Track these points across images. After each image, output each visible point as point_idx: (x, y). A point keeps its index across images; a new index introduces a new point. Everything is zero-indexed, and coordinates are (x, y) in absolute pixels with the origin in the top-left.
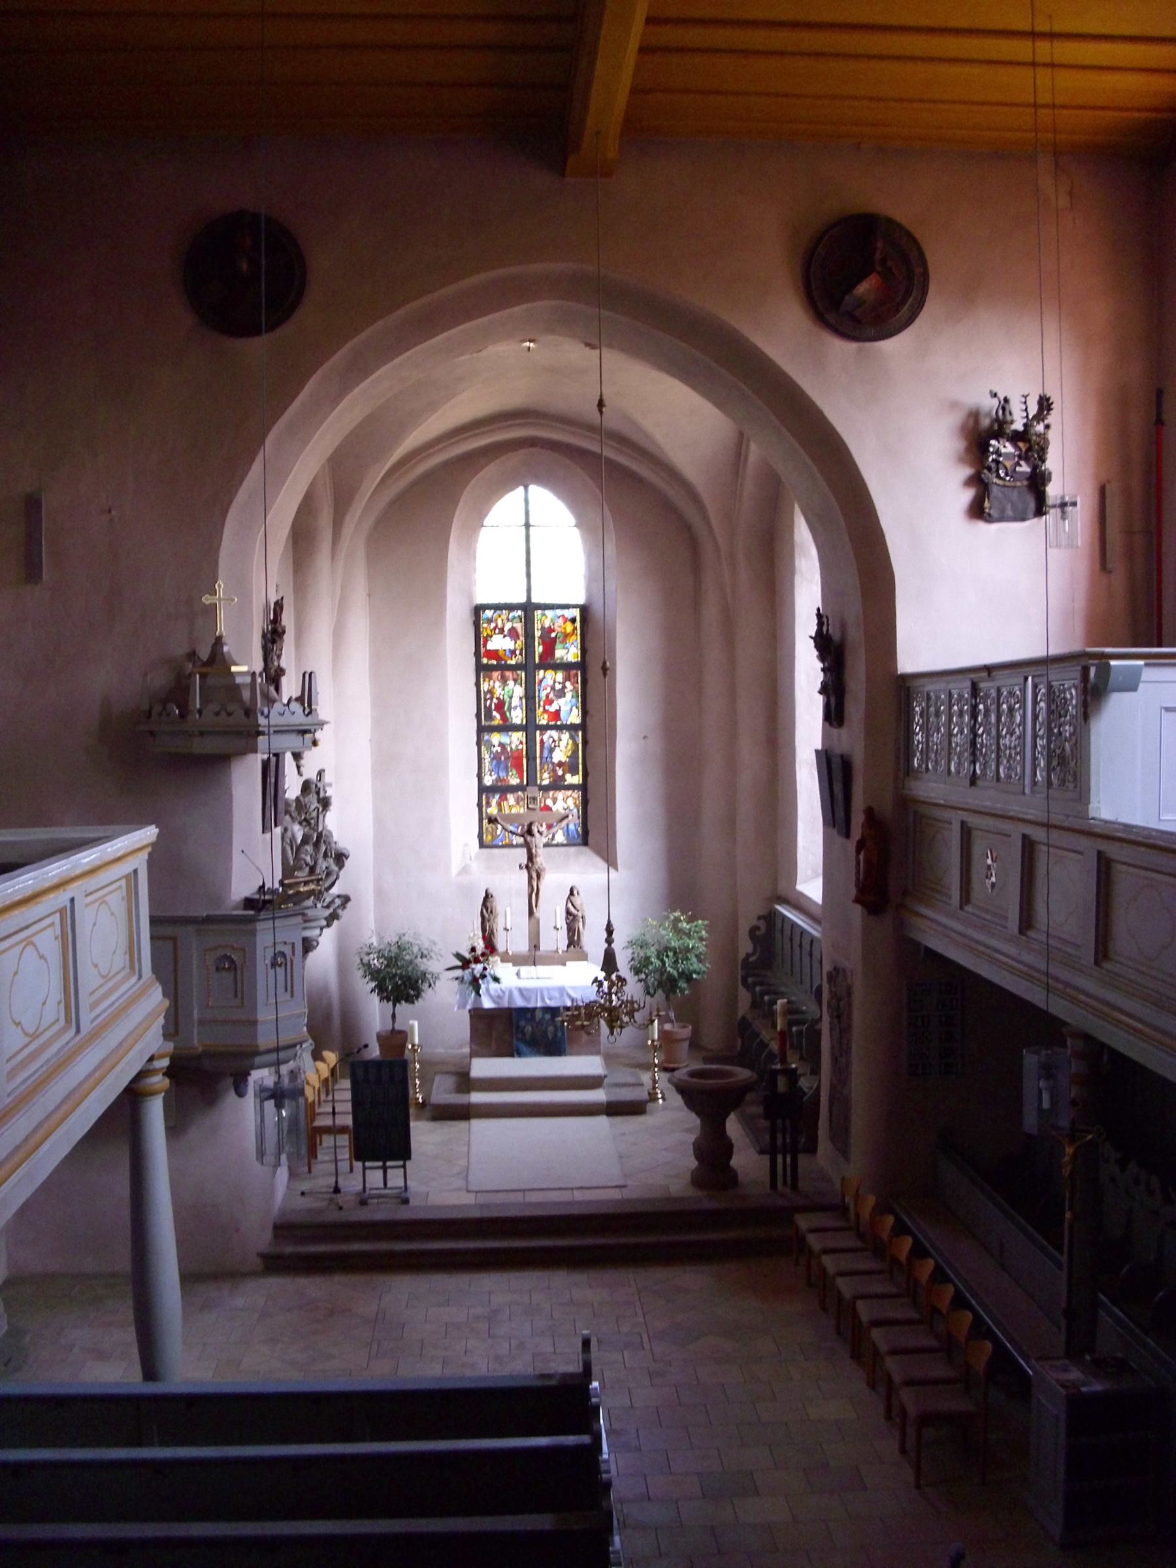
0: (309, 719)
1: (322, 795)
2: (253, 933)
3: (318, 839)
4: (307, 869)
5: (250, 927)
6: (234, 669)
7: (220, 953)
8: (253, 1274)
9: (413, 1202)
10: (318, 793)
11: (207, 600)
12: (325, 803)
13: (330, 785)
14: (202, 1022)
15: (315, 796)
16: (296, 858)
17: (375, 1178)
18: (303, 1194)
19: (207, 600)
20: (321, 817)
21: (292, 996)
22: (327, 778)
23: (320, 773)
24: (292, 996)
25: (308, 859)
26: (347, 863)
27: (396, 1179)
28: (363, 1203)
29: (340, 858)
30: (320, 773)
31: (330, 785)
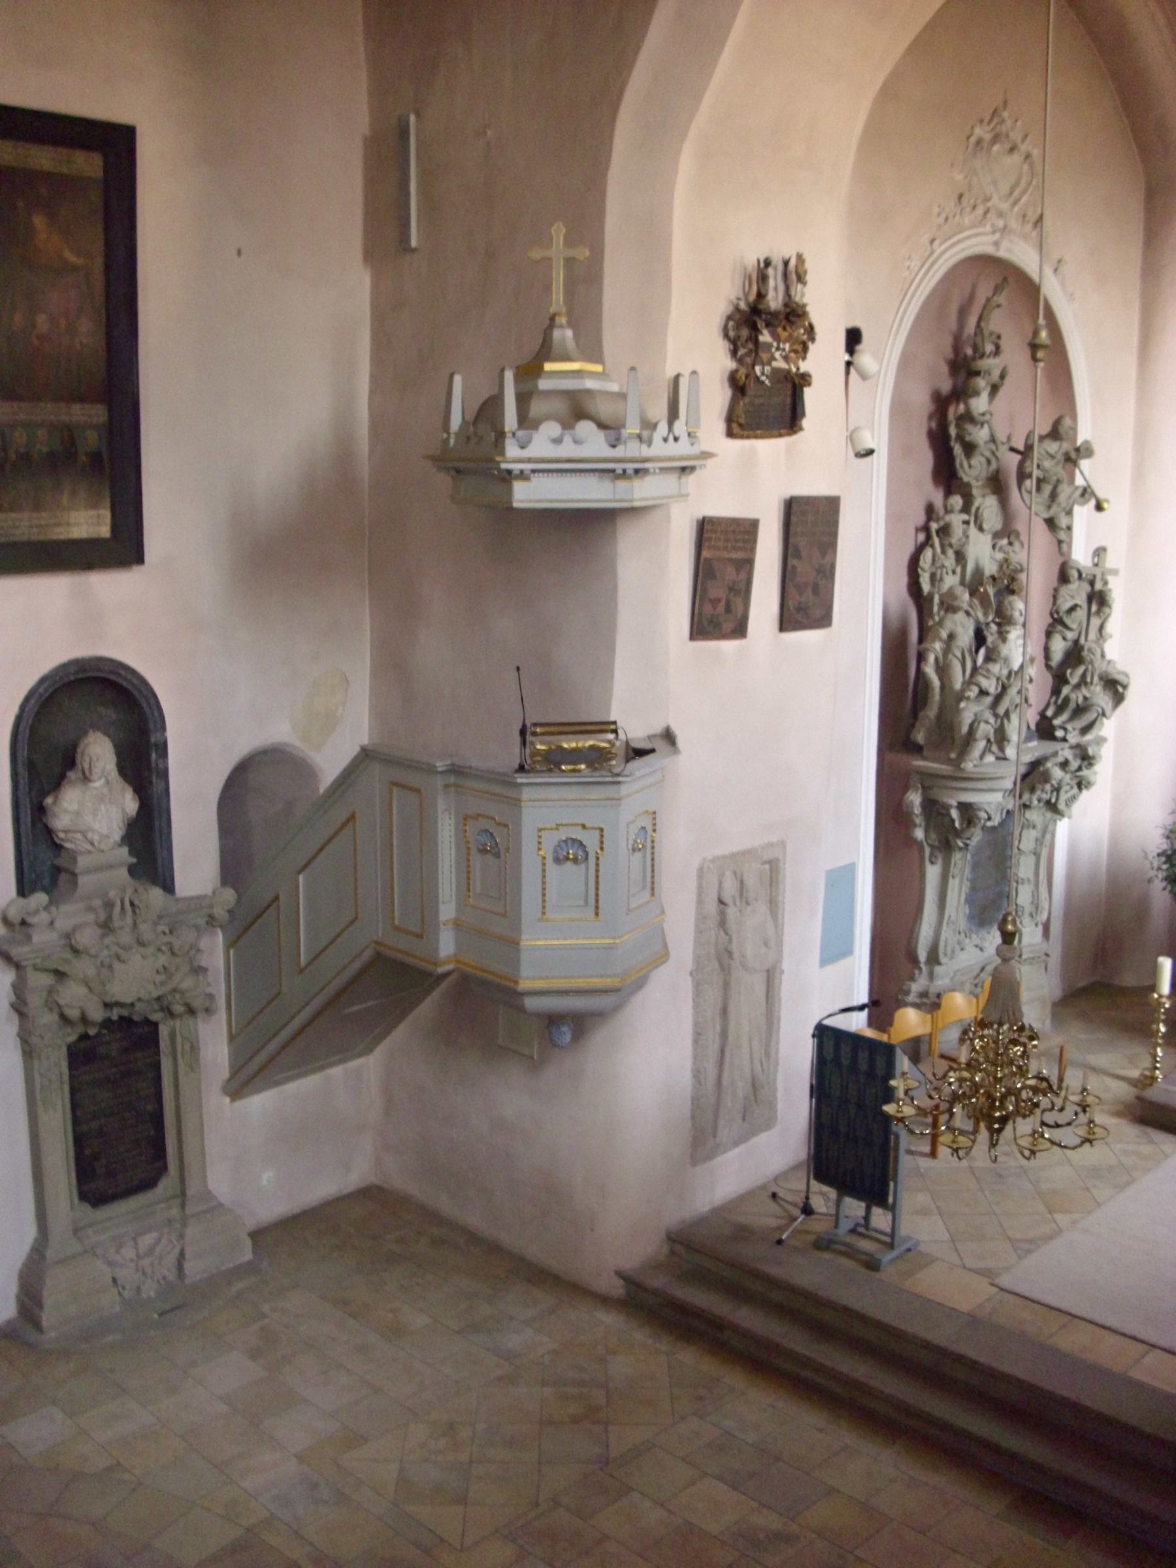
0: (619, 452)
1: (1098, 586)
2: (516, 803)
3: (1075, 655)
4: (988, 700)
5: (511, 793)
6: (548, 366)
7: (483, 824)
8: (604, 1300)
9: (888, 1273)
10: (1092, 583)
11: (536, 254)
12: (1099, 599)
13: (1115, 572)
14: (457, 924)
15: (1088, 588)
16: (968, 683)
17: (854, 1207)
18: (774, 1195)
19: (536, 254)
20: (1095, 622)
21: (597, 914)
22: (1110, 562)
23: (1100, 552)
24: (597, 914)
25: (991, 686)
26: (1131, 695)
27: (880, 1219)
28: (824, 1244)
29: (1115, 688)
30: (1100, 552)
31: (1115, 572)
